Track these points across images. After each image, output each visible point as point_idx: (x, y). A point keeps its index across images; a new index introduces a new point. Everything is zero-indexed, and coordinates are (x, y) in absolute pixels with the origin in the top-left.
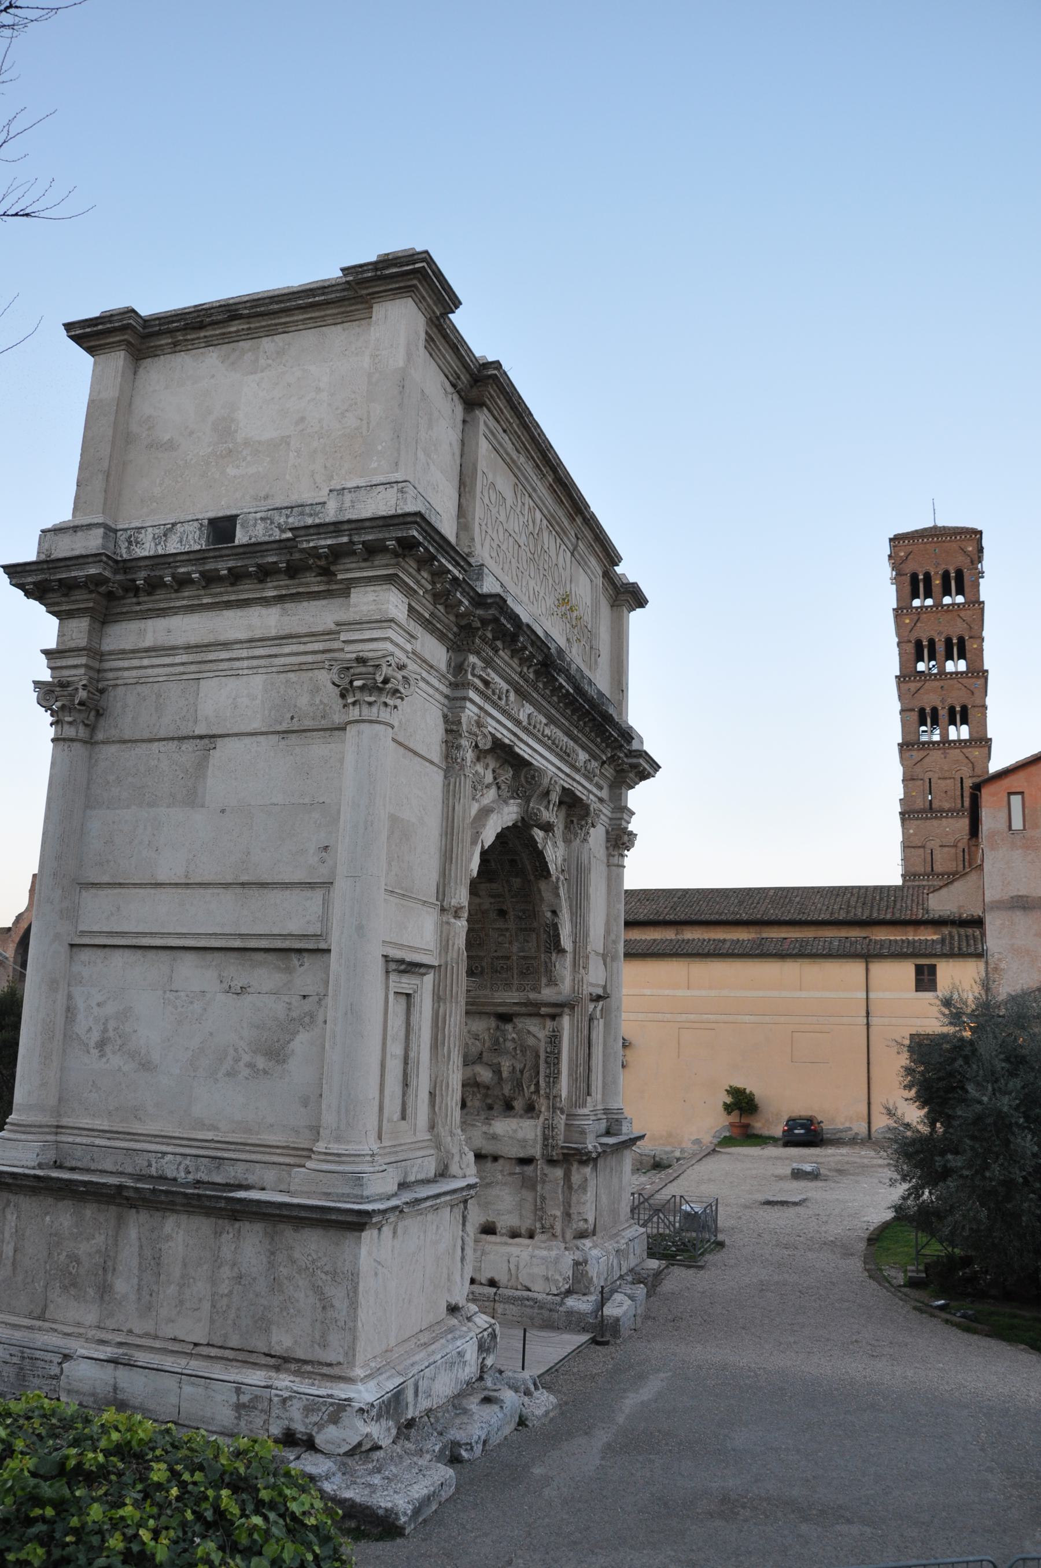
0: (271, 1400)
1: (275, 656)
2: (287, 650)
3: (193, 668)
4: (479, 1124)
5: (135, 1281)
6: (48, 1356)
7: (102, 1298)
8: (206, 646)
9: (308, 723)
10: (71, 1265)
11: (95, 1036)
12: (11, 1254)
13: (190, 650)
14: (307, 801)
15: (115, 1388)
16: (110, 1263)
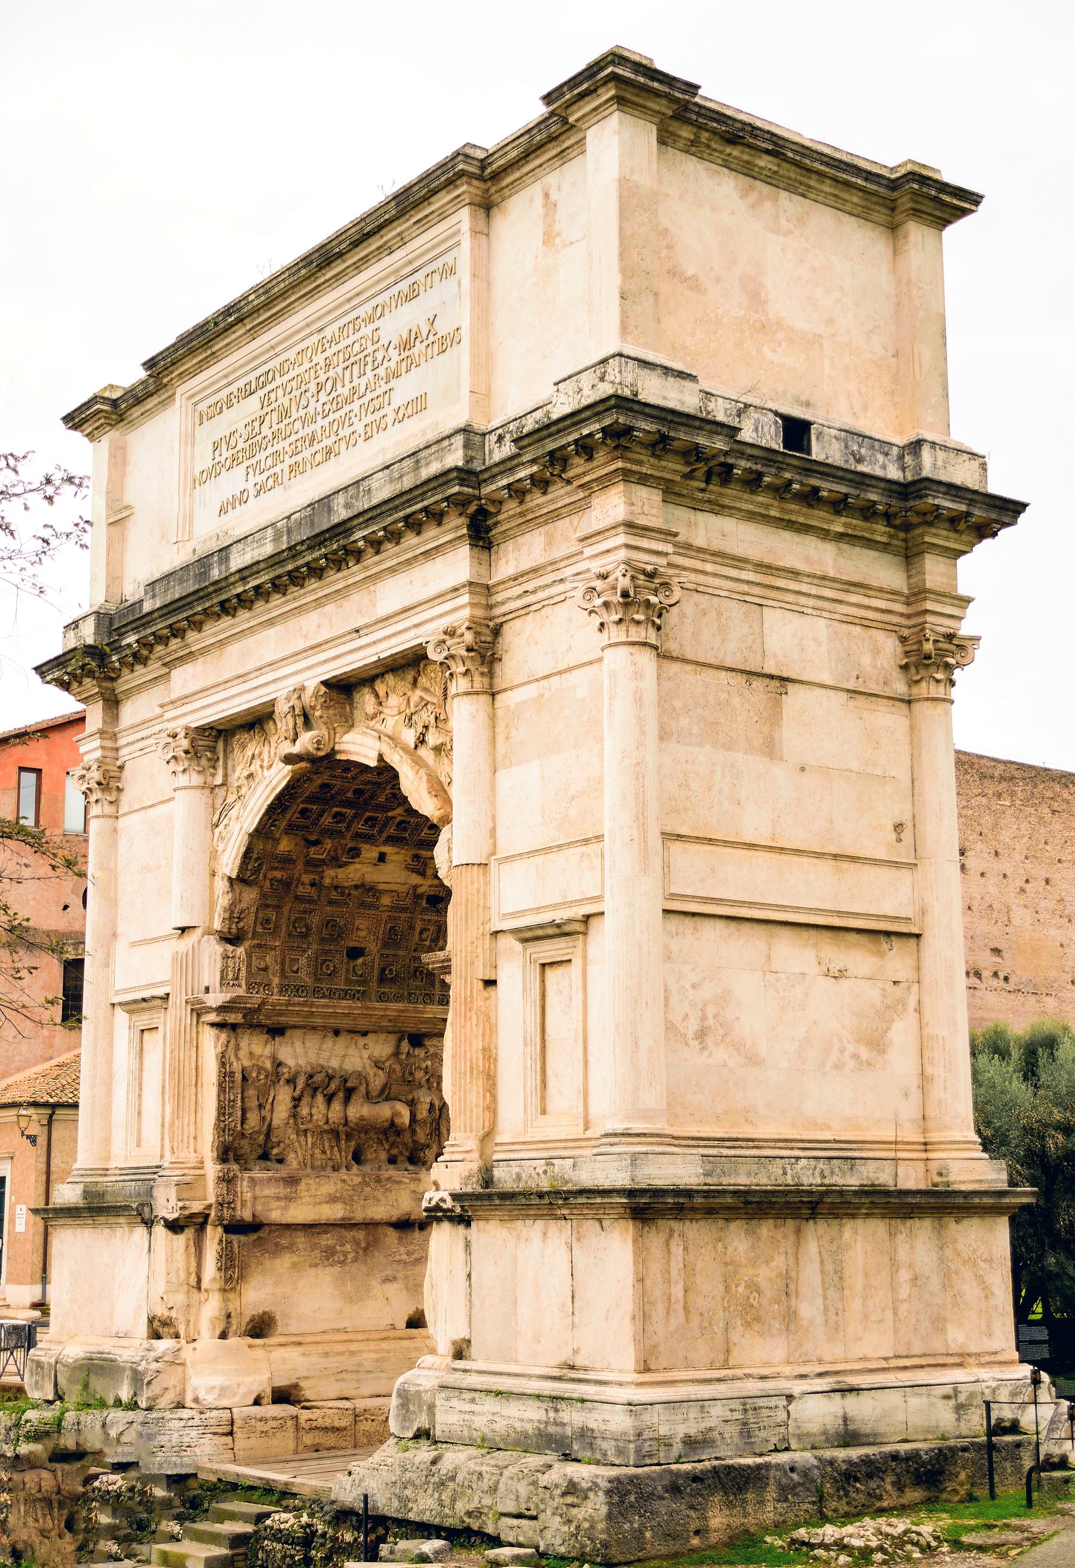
0: (983, 1393)
1: (840, 602)
2: (853, 598)
3: (757, 590)
4: (407, 1181)
5: (820, 1302)
6: (773, 1402)
7: (788, 1329)
8: (777, 569)
9: (873, 688)
10: (752, 1296)
11: (693, 1025)
12: (681, 1294)
13: (759, 569)
14: (879, 772)
15: (845, 1419)
16: (792, 1287)
